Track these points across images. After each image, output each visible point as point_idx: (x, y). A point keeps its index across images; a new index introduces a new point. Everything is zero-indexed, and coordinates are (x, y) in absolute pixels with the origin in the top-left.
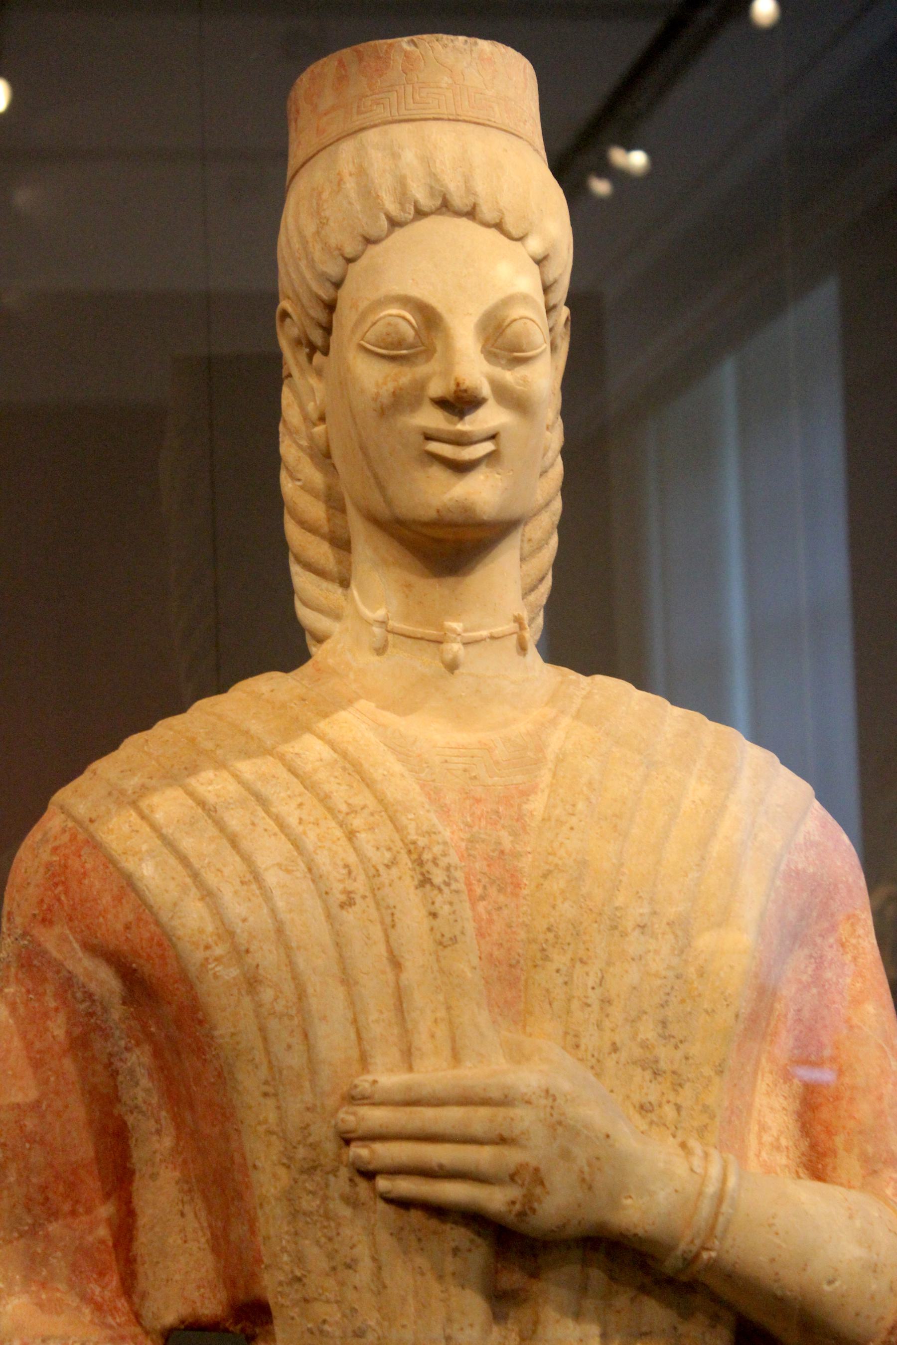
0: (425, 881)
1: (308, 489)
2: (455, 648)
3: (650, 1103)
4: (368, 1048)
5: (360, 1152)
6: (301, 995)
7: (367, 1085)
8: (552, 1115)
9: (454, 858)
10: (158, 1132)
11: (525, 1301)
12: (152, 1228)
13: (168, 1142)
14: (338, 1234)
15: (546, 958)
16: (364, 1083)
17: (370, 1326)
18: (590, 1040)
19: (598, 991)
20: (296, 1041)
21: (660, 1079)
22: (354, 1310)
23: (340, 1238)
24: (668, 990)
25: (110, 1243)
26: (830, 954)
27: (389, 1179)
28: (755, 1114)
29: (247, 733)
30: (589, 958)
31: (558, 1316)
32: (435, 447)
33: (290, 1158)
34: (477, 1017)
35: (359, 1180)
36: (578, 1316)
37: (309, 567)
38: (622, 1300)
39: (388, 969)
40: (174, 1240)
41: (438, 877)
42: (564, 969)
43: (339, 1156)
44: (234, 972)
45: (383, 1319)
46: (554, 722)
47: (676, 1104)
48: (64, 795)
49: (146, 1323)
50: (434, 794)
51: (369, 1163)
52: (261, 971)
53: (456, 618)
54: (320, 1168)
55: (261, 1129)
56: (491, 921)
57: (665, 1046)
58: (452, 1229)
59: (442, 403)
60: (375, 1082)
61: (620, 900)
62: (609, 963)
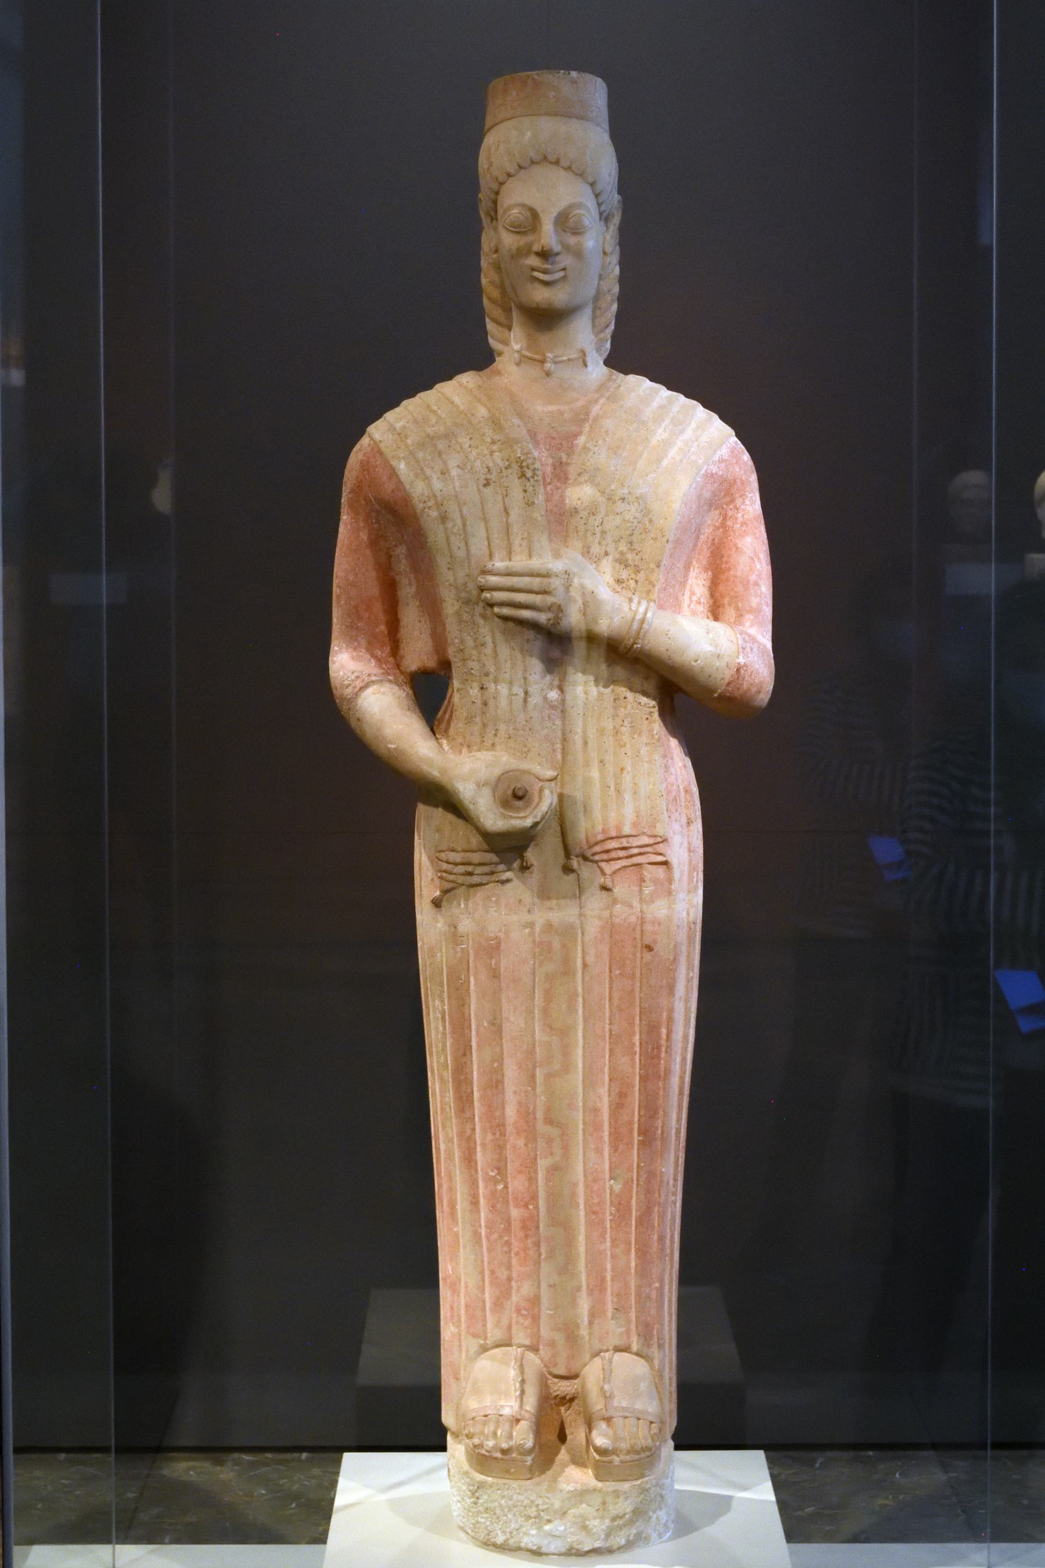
0: (523, 475)
1: (492, 283)
2: (548, 365)
5: (487, 595)
6: (464, 525)
9: (538, 465)
13: (414, 589)
16: (489, 566)
18: (596, 549)
20: (462, 545)
26: (730, 513)
28: (688, 587)
29: (452, 402)
32: (536, 274)
36: (584, 672)
37: (493, 320)
41: (529, 474)
43: (479, 596)
46: (596, 401)
48: (371, 429)
49: (402, 668)
50: (533, 435)
53: (551, 351)
56: (552, 494)
59: (538, 254)
61: (613, 487)
62: (607, 515)
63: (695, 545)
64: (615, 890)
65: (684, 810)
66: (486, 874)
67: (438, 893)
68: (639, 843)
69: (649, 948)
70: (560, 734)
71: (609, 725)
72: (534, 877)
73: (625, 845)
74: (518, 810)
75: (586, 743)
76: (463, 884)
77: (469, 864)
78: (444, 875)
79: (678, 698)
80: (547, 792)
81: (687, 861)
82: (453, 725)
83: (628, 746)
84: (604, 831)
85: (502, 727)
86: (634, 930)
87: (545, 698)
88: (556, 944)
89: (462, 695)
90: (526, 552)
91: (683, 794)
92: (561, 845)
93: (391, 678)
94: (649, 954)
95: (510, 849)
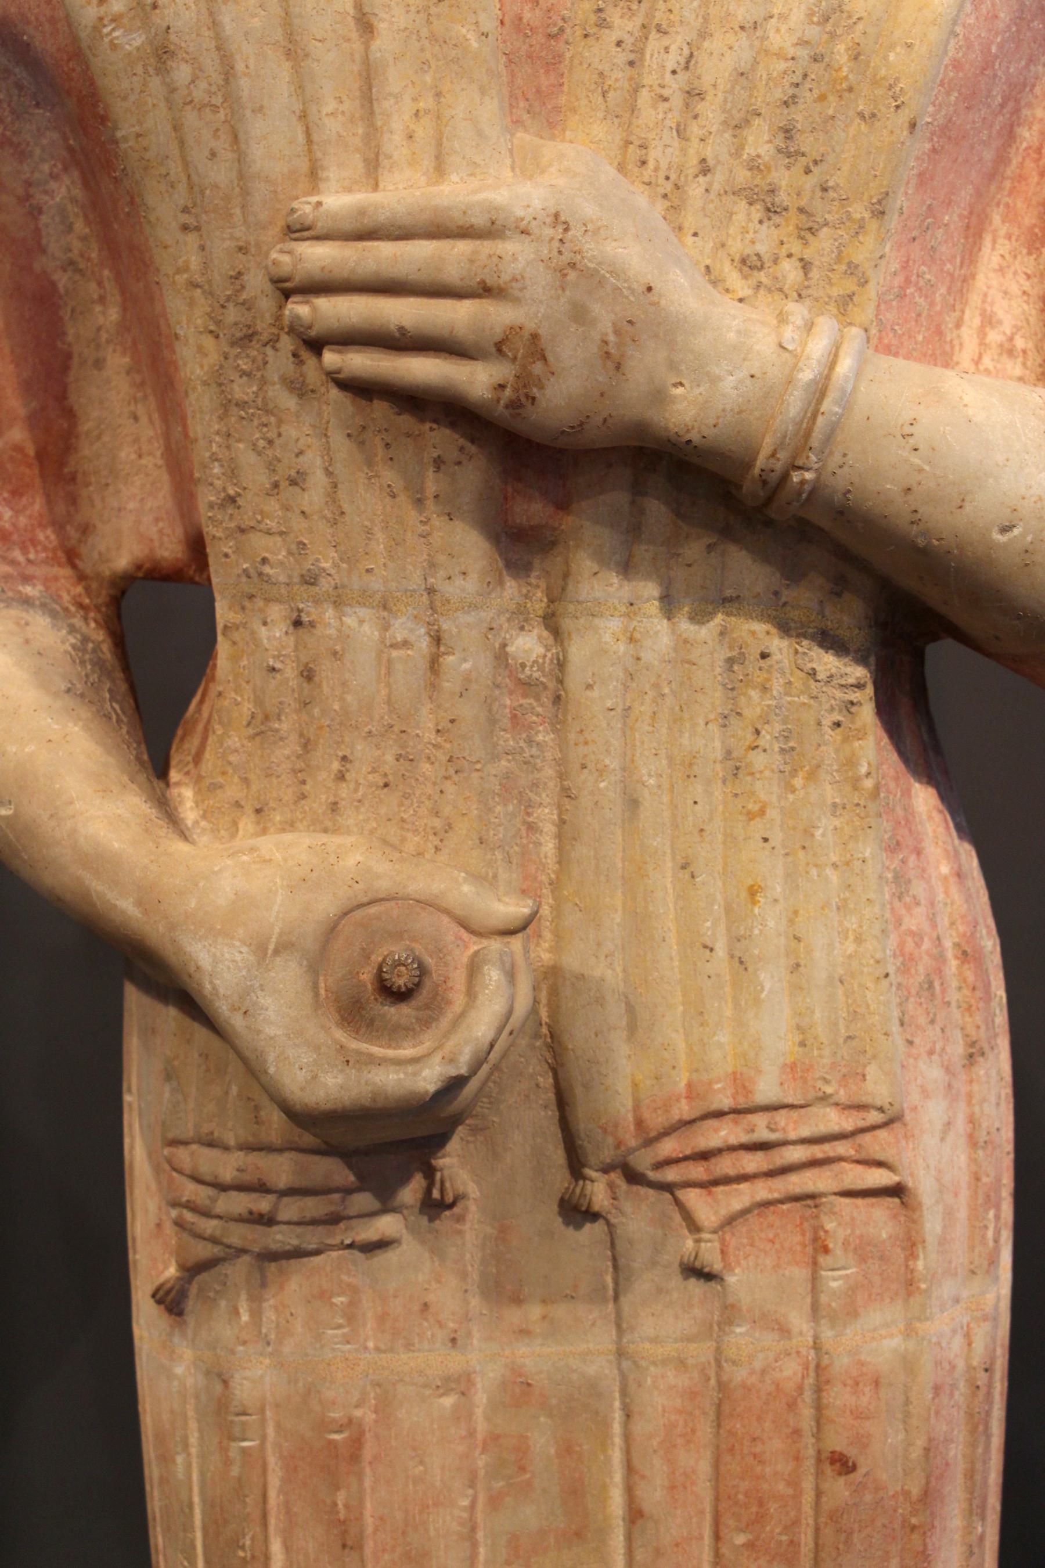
3: (758, 255)
4: (319, 155)
6: (228, 73)
7: (308, 209)
8: (560, 252)
10: (102, 299)
11: (554, 544)
12: (99, 437)
13: (114, 314)
14: (280, 435)
15: (603, 24)
16: (305, 208)
17: (324, 570)
18: (664, 152)
19: (682, 77)
20: (222, 144)
21: (777, 219)
22: (302, 545)
23: (282, 440)
24: (797, 78)
25: (31, 451)
27: (340, 352)
28: (975, 299)
30: (671, 24)
31: (596, 568)
33: (218, 323)
34: (477, 108)
35: (305, 354)
36: (627, 568)
38: (694, 550)
39: (354, 35)
40: (127, 454)
42: (629, 40)
44: (138, 40)
45: (342, 560)
47: (801, 260)
51: (310, 327)
52: (173, 37)
54: (256, 338)
55: (181, 279)
57: (788, 168)
58: (431, 429)
60: (319, 204)
62: (704, 34)
63: (1002, 159)
64: (731, 1279)
65: (956, 1015)
66: (314, 1222)
67: (172, 1271)
68: (805, 1132)
69: (844, 1465)
70: (549, 772)
71: (708, 743)
72: (472, 1229)
73: (763, 1134)
74: (395, 1033)
75: (633, 804)
76: (242, 1251)
77: (261, 1188)
78: (189, 1216)
79: (943, 657)
80: (493, 975)
81: (964, 1178)
82: (211, 740)
83: (772, 813)
84: (692, 1092)
85: (361, 749)
86: (792, 1406)
87: (501, 656)
88: (542, 1442)
89: (250, 644)
90: (428, 163)
91: (953, 964)
92: (555, 1130)
93: (28, 590)
94: (842, 1480)
95: (387, 1151)
